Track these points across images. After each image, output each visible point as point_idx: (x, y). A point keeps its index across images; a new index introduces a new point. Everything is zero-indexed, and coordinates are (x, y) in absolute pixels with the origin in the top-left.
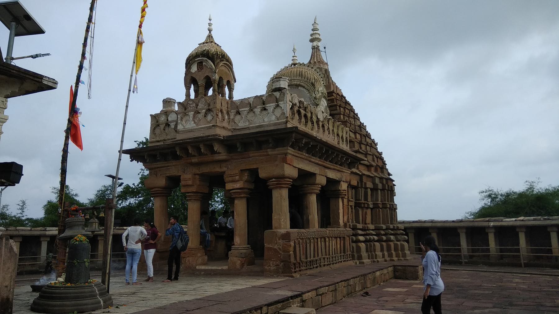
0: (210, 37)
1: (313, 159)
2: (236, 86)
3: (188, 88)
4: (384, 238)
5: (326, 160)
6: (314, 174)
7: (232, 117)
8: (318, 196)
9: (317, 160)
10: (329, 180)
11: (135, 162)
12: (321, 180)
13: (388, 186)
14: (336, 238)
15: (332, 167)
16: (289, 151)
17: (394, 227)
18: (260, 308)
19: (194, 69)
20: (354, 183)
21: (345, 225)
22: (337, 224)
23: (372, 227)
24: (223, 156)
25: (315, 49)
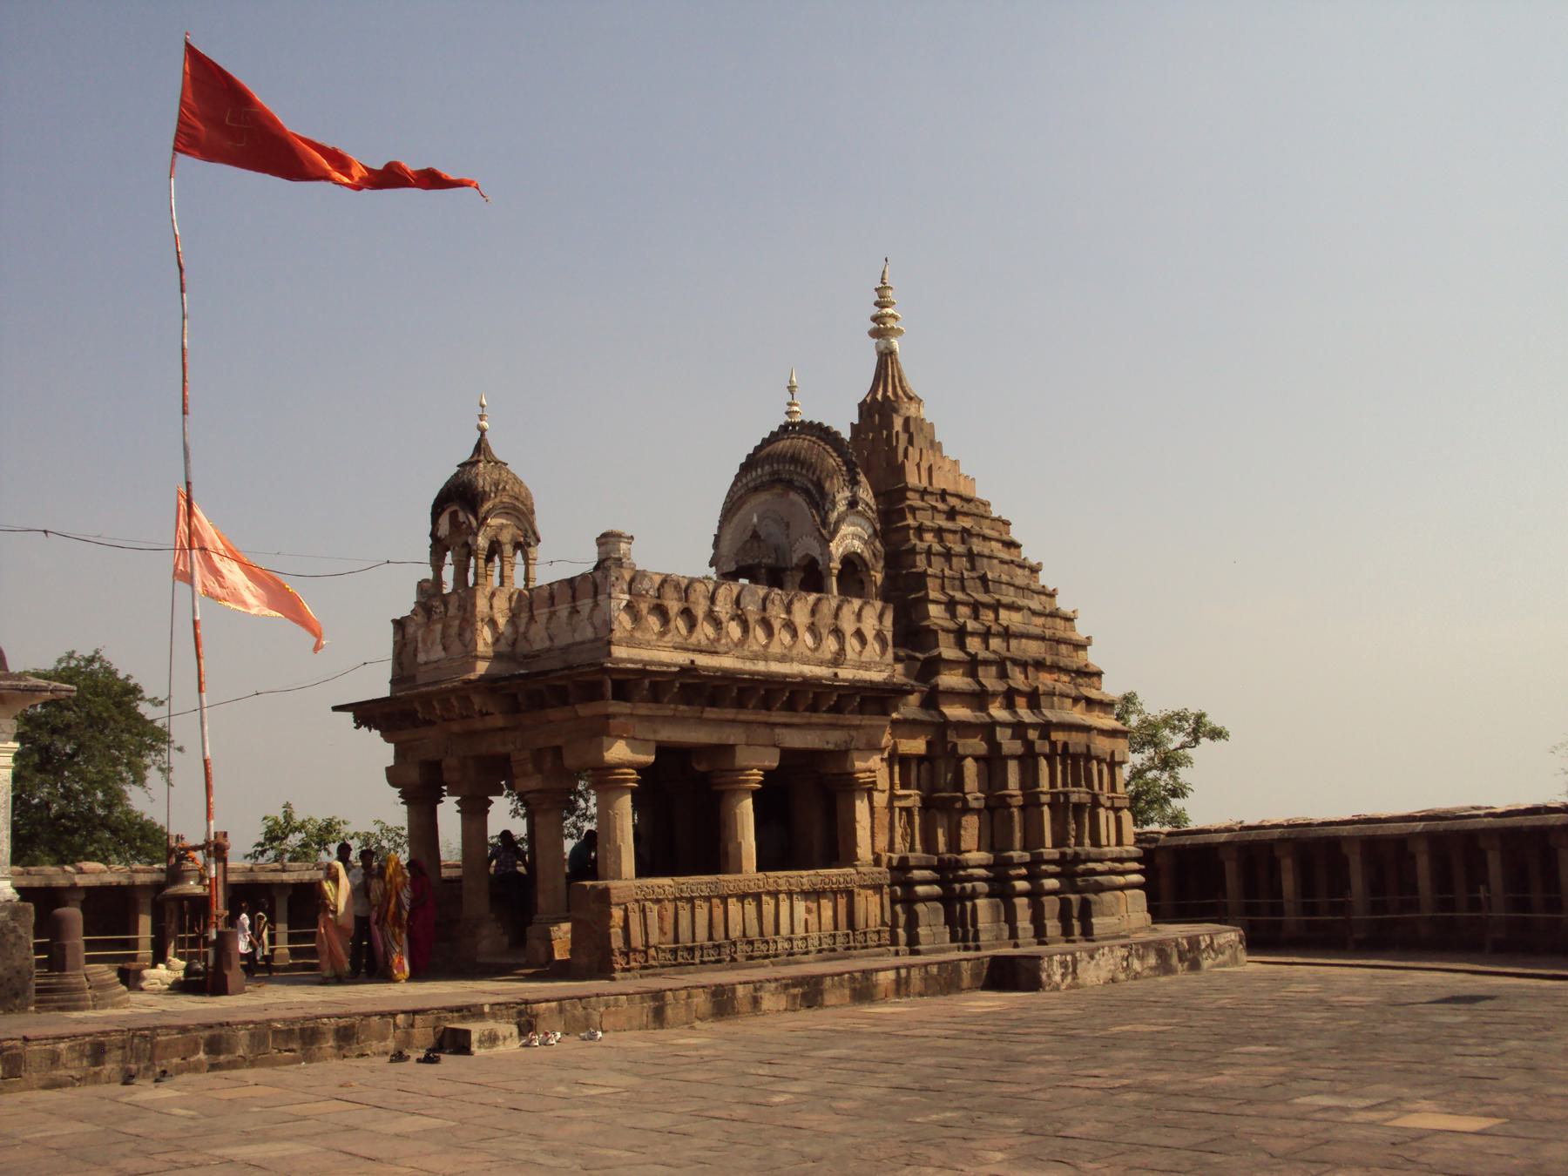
0: (481, 448)
1: (711, 713)
2: (539, 552)
3: (437, 566)
4: (1021, 885)
5: (769, 709)
6: (728, 750)
7: (522, 629)
8: (757, 796)
9: (730, 713)
10: (787, 754)
11: (364, 729)
12: (756, 763)
13: (1053, 744)
14: (835, 893)
15: (796, 720)
16: (611, 710)
17: (1063, 854)
18: (393, 1014)
19: (444, 521)
20: (917, 746)
21: (877, 861)
22: (850, 858)
23: (976, 856)
24: (499, 721)
25: (886, 359)
